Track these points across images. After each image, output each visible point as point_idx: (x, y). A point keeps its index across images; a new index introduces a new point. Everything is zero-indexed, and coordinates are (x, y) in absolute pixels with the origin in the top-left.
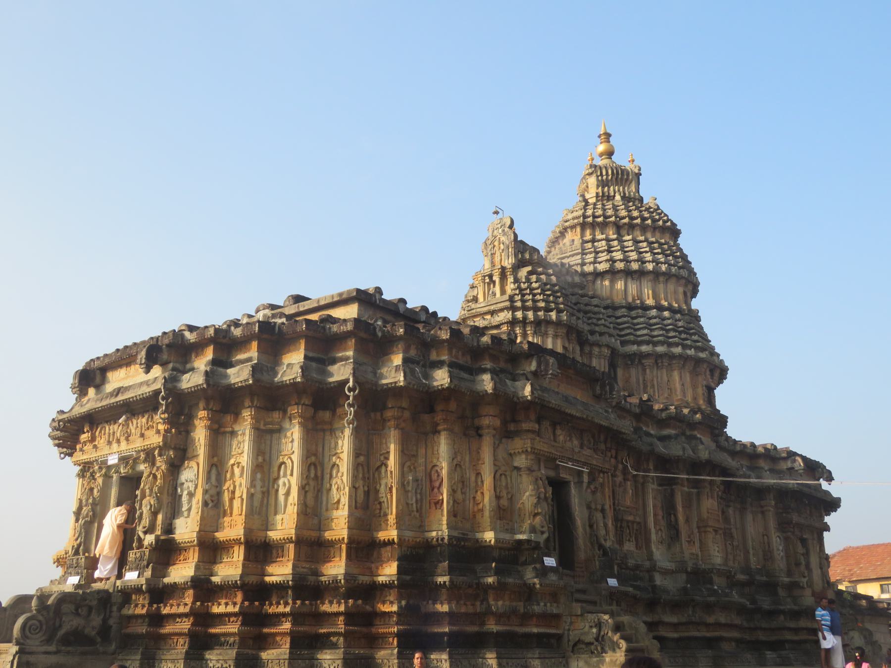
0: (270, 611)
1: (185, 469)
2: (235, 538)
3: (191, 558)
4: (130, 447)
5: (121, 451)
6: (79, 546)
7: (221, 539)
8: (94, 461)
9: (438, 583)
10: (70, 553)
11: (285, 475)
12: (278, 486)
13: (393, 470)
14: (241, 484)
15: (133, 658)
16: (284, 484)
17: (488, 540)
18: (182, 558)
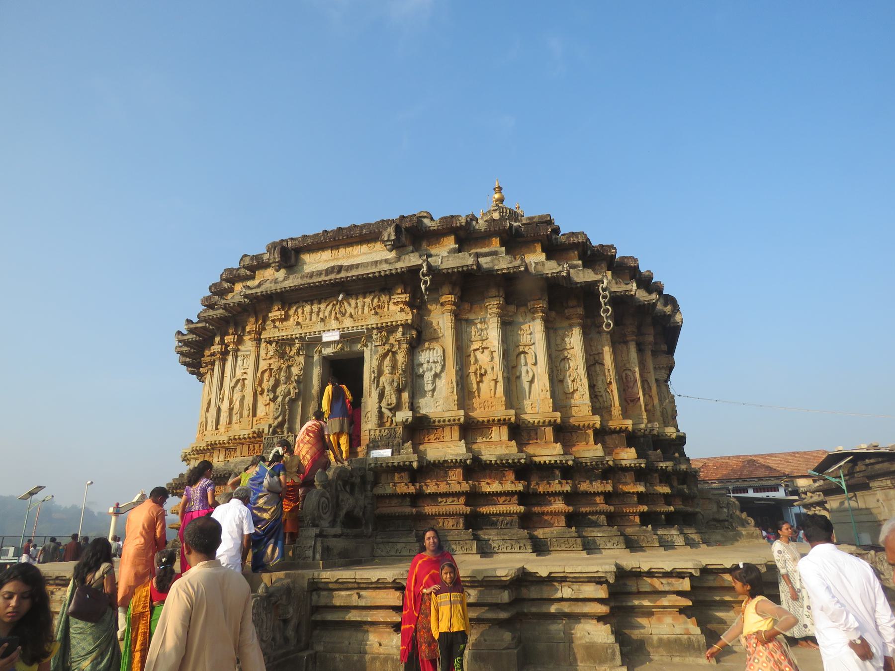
0: (541, 489)
1: (422, 351)
2: (502, 418)
3: (448, 438)
4: (356, 325)
5: (344, 328)
6: (281, 425)
7: (481, 420)
8: (297, 338)
9: (659, 468)
10: (266, 431)
11: (526, 364)
12: (521, 374)
13: (610, 368)
14: (493, 368)
15: (403, 540)
16: (527, 372)
17: (669, 434)
18: (432, 437)
